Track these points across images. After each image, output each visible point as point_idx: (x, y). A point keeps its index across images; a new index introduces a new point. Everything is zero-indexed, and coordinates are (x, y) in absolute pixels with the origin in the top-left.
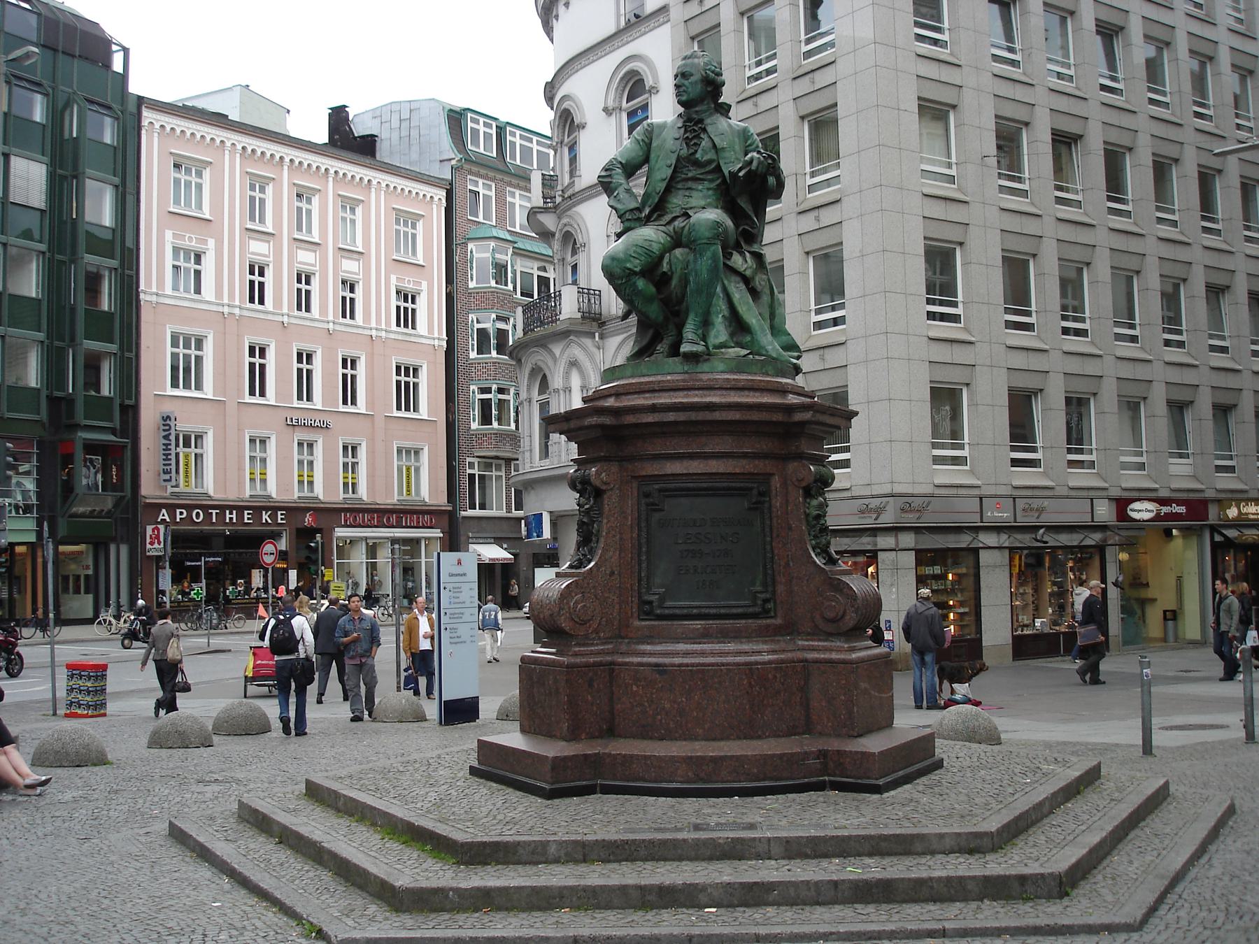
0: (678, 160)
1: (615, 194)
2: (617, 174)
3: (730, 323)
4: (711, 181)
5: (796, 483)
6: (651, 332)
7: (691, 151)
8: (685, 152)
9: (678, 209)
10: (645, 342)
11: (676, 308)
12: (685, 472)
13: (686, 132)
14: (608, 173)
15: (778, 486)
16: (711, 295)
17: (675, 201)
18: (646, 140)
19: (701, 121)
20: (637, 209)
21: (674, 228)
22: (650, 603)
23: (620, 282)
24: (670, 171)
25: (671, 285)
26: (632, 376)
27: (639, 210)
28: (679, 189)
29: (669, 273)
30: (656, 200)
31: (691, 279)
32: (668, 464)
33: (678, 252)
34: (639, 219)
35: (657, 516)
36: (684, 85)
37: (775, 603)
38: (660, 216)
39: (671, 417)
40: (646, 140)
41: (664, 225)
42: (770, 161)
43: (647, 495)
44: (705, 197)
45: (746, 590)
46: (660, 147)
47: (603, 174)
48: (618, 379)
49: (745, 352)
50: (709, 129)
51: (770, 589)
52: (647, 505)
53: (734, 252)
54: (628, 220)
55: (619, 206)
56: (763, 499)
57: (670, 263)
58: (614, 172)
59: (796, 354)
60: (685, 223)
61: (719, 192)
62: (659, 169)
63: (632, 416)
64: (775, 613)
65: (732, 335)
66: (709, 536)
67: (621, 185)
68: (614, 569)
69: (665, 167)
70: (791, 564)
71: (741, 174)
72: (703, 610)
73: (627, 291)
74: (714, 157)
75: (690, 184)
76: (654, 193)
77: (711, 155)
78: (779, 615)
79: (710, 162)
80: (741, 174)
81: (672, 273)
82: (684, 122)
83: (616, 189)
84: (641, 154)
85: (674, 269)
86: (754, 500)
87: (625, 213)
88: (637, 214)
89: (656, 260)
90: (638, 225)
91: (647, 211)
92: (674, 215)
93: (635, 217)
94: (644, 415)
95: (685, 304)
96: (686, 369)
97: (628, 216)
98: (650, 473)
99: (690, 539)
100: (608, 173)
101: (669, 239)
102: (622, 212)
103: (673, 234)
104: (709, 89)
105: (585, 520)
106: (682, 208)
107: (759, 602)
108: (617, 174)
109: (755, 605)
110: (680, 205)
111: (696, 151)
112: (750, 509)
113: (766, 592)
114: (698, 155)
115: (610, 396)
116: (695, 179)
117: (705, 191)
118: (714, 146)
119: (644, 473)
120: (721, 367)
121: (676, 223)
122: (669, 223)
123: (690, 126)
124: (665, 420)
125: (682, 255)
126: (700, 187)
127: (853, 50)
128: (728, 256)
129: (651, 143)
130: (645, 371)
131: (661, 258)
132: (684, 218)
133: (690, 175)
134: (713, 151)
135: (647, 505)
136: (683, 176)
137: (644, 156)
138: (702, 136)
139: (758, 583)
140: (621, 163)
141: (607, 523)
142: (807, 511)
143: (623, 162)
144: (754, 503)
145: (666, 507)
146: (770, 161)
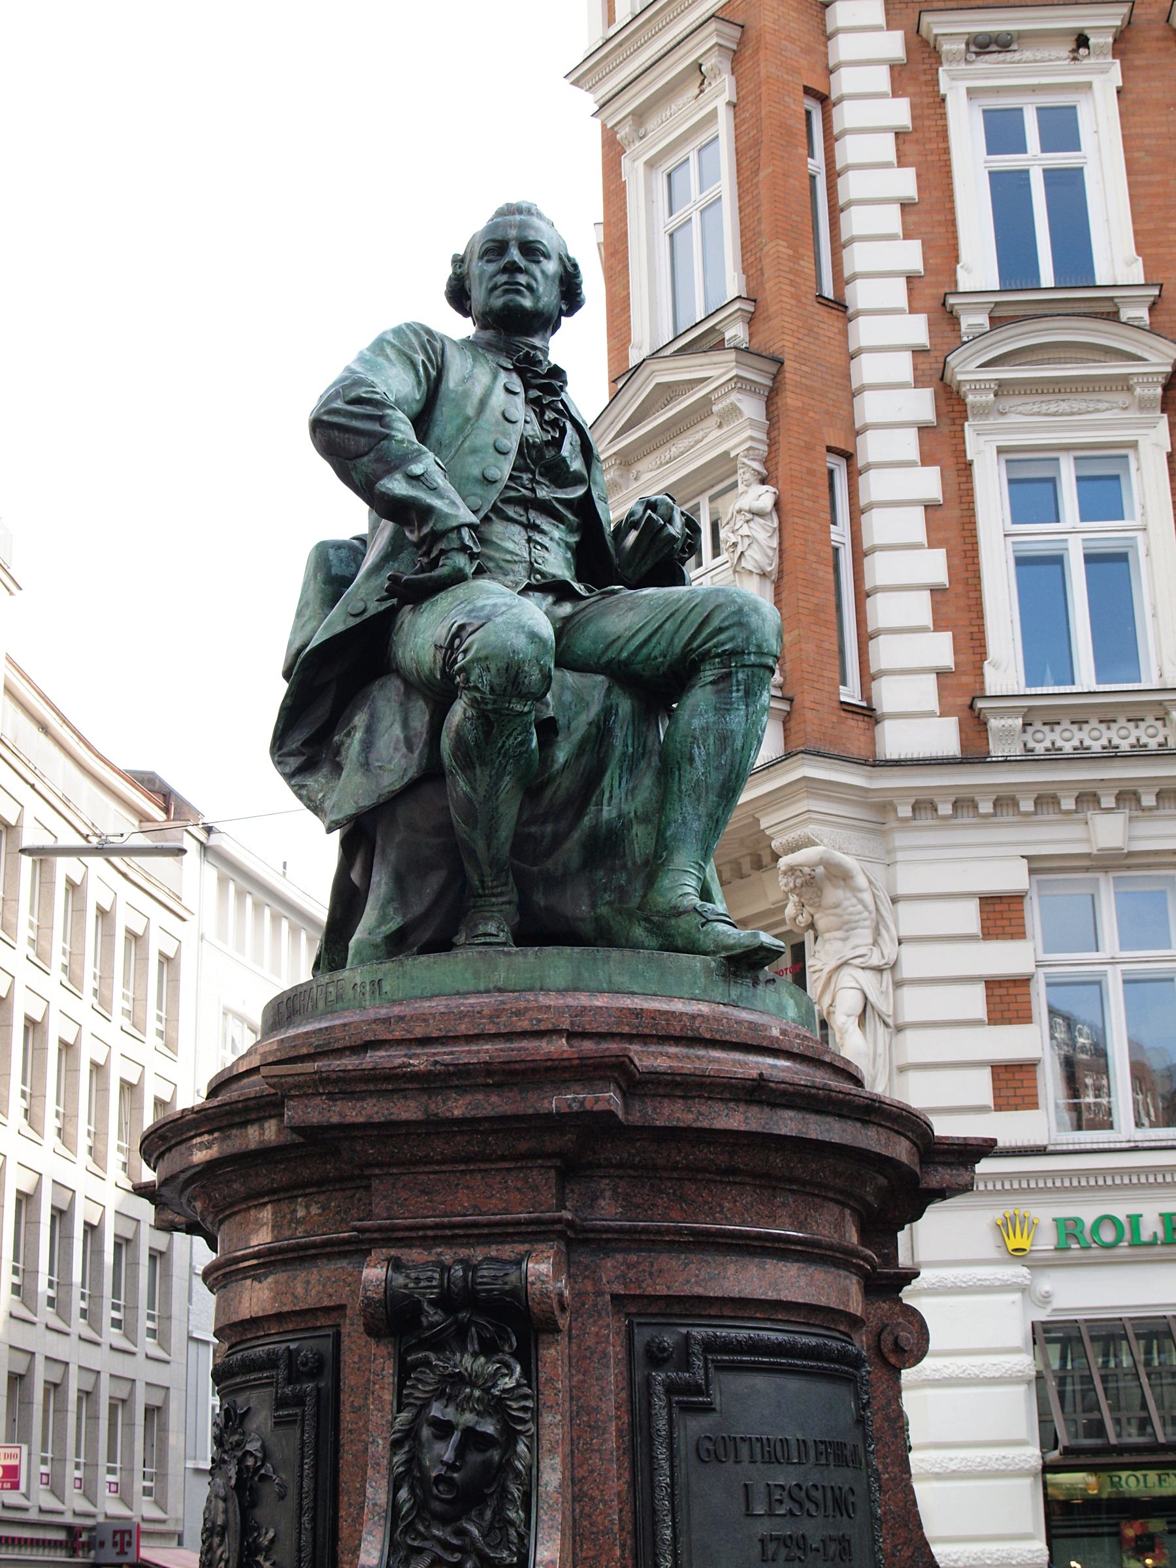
4: (571, 530)
5: (893, 1360)
8: (534, 430)
12: (771, 1295)
32: (731, 1270)
35: (696, 1426)
39: (788, 1123)
43: (656, 1357)
52: (671, 1389)
63: (680, 1104)
79: (577, 479)
87: (459, 528)
94: (718, 1106)
98: (678, 1289)
105: (489, 1427)
119: (662, 1290)
124: (775, 1132)
126: (557, 534)
130: (622, 980)
135: (671, 1389)
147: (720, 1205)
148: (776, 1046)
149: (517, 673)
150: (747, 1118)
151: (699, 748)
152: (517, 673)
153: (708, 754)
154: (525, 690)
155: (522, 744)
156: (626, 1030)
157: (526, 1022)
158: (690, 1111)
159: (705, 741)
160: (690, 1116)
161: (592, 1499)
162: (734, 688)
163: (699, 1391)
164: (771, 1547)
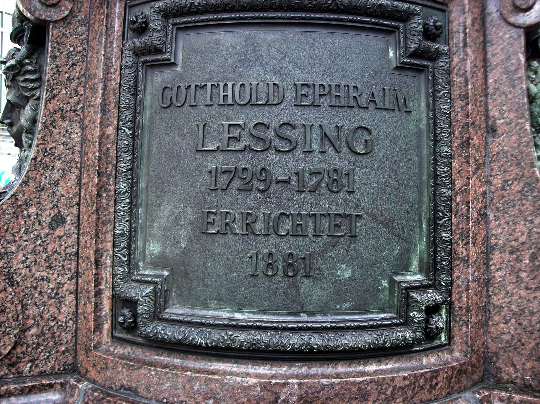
15: (469, 22)
22: (132, 303)
37: (450, 313)
45: (385, 283)
51: (444, 278)
56: (435, 46)
64: (450, 338)
66: (287, 132)
68: (64, 212)
70: (491, 217)
72: (264, 337)
78: (457, 339)
86: (413, 46)
99: (237, 139)
107: (417, 315)
109: (407, 322)
112: (401, 68)
113: (434, 285)
139: (415, 264)
141: (48, 101)
142: (532, 86)
144: (414, 55)
145: (180, 56)
161: (89, 141)
163: (159, 51)
164: (223, 180)
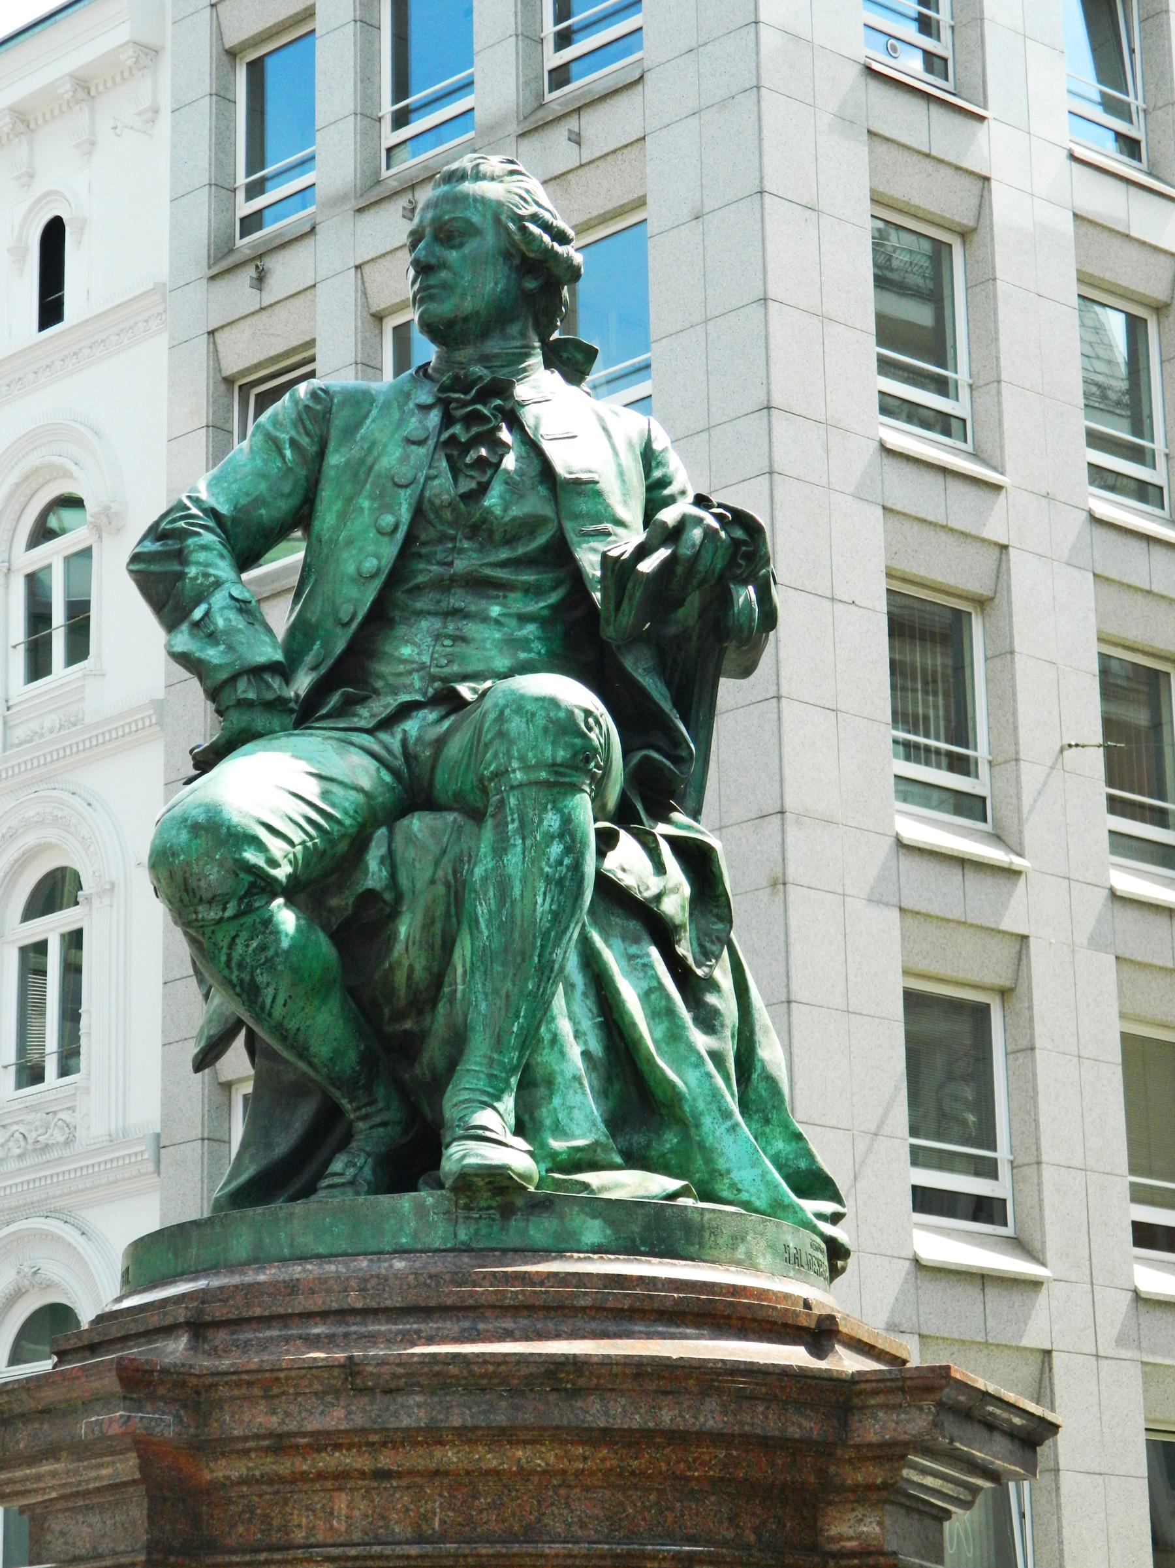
0: (418, 512)
1: (198, 614)
2: (204, 548)
3: (609, 1080)
6: (306, 1112)
7: (466, 485)
8: (444, 487)
9: (416, 681)
10: (283, 1145)
11: (408, 1025)
13: (447, 420)
14: (172, 545)
16: (547, 972)
17: (406, 651)
18: (305, 441)
19: (503, 389)
20: (273, 667)
21: (404, 742)
23: (213, 914)
24: (389, 551)
25: (392, 938)
26: (258, 1260)
27: (284, 670)
28: (420, 614)
29: (388, 896)
30: (340, 646)
31: (482, 910)
33: (418, 823)
34: (277, 705)
36: (443, 265)
38: (346, 708)
40: (305, 441)
41: (369, 732)
42: (739, 534)
44: (512, 643)
46: (360, 471)
47: (150, 546)
48: (196, 1274)
49: (674, 1184)
50: (528, 416)
53: (624, 835)
54: (244, 704)
55: (213, 654)
57: (390, 859)
58: (191, 541)
59: (829, 1207)
60: (446, 724)
61: (560, 628)
62: (349, 542)
65: (615, 1123)
67: (218, 584)
69: (372, 534)
71: (647, 566)
73: (239, 949)
74: (547, 511)
75: (458, 599)
76: (329, 623)
77: (535, 504)
79: (531, 525)
80: (647, 566)
81: (399, 898)
82: (443, 389)
83: (201, 596)
84: (287, 488)
85: (404, 881)
87: (234, 679)
88: (276, 683)
89: (343, 847)
90: (276, 723)
91: (303, 683)
92: (405, 698)
93: (270, 696)
95: (442, 1008)
96: (463, 1235)
97: (245, 690)
100: (172, 545)
101: (387, 777)
102: (224, 675)
103: (399, 763)
104: (531, 284)
106: (433, 678)
108: (204, 548)
110: (423, 667)
111: (483, 488)
114: (493, 500)
115: (168, 1330)
116: (480, 585)
117: (513, 623)
118: (546, 471)
120: (593, 1231)
121: (411, 726)
122: (387, 723)
123: (465, 404)
125: (434, 833)
126: (495, 611)
127: (703, 425)
128: (607, 841)
129: (321, 454)
130: (307, 1242)
131: (359, 842)
132: (441, 711)
133: (461, 565)
134: (542, 490)
136: (435, 568)
137: (295, 501)
138: (505, 435)
140: (213, 513)
143: (224, 509)
146: (739, 534)
147: (384, 1518)
148: (471, 1302)
149: (185, 879)
150: (350, 1413)
151: (481, 904)
152: (185, 879)
153: (490, 911)
154: (207, 895)
155: (263, 948)
156: (258, 1312)
157: (156, 1318)
158: (274, 1413)
159: (485, 894)
160: (274, 1419)
162: (509, 819)
